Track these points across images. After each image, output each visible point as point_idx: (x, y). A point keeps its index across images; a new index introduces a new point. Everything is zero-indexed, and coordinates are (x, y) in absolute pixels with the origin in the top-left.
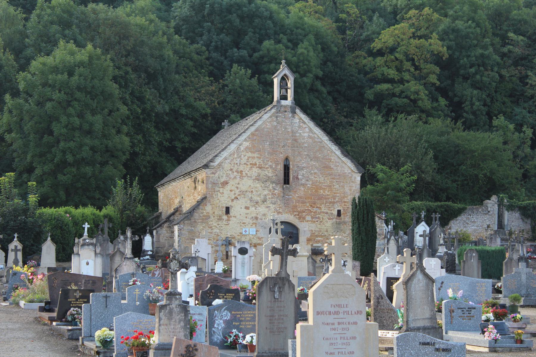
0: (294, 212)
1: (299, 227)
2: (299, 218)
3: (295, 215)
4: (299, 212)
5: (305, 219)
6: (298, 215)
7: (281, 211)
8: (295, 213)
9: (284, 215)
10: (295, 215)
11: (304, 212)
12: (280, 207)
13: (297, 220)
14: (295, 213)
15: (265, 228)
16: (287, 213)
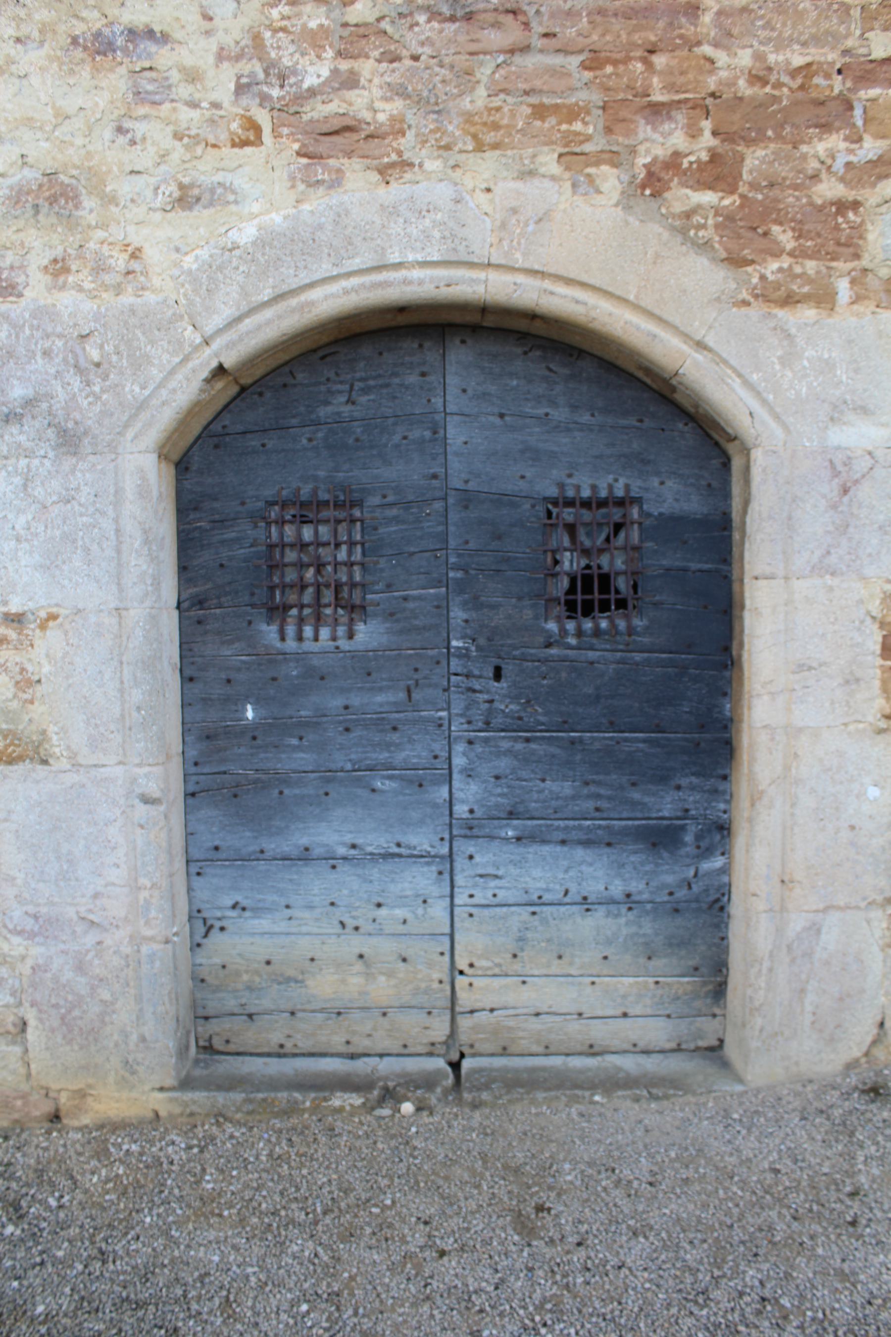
0: (631, 108)
1: (728, 394)
2: (742, 237)
3: (654, 182)
4: (739, 120)
5: (850, 246)
6: (718, 172)
7: (372, 102)
8: (658, 141)
9: (430, 183)
10: (654, 182)
11: (831, 114)
12: (354, 40)
13: (699, 278)
14: (658, 141)
15: (69, 440)
16: (486, 135)
